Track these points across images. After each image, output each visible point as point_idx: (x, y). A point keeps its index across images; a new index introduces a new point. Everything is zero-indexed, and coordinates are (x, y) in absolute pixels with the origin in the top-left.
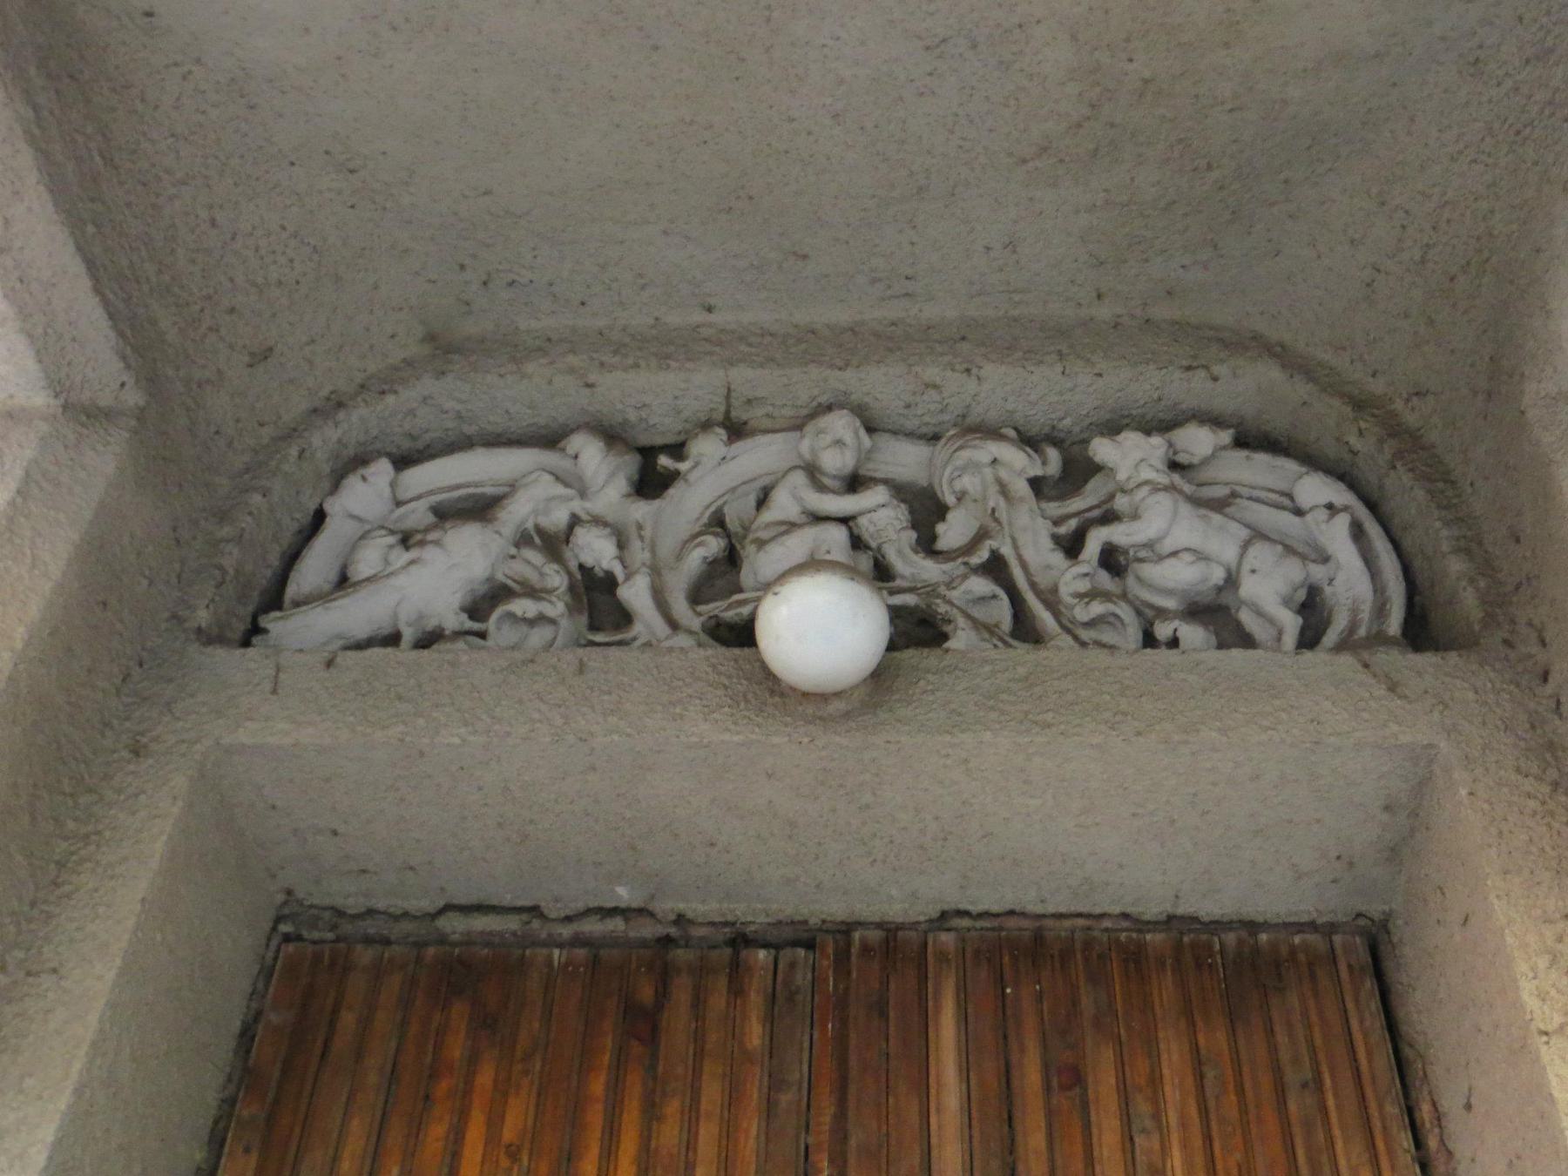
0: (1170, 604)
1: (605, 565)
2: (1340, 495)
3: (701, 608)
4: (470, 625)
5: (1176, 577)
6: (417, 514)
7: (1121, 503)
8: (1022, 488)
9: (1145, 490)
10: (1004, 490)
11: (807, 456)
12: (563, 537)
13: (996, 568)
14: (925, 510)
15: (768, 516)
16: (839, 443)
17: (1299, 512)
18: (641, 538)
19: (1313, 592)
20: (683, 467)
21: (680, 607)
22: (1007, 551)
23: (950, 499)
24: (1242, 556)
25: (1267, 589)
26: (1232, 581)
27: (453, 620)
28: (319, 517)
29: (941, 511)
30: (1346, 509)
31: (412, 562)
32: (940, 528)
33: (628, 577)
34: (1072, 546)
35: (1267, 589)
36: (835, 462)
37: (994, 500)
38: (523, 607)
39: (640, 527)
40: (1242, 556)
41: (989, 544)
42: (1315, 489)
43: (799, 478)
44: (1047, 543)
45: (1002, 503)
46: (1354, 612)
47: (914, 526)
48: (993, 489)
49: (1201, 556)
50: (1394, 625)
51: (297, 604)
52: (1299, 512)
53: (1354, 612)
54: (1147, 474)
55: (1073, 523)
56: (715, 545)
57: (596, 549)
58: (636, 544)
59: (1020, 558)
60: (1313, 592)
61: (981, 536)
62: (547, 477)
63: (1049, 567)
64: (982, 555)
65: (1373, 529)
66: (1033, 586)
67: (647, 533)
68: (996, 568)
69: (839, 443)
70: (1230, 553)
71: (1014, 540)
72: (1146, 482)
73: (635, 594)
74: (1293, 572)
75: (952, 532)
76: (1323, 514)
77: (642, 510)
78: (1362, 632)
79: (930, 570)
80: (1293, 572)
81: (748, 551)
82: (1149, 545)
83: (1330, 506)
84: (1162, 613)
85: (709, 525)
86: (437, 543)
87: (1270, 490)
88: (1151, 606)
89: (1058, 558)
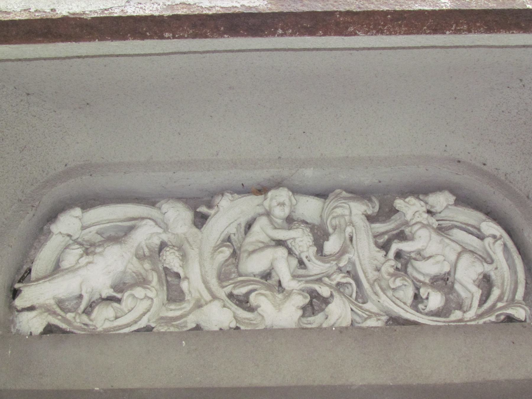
0: (427, 281)
5: (429, 268)
6: (91, 234)
11: (267, 208)
14: (320, 235)
15: (251, 238)
16: (282, 204)
20: (212, 212)
21: (214, 282)
30: (501, 237)
36: (280, 213)
42: (490, 228)
43: (263, 221)
47: (315, 245)
51: (38, 280)
52: (481, 237)
56: (227, 252)
69: (282, 204)
70: (453, 257)
74: (479, 268)
80: (479, 268)
82: (419, 253)
85: (224, 241)
88: (419, 281)
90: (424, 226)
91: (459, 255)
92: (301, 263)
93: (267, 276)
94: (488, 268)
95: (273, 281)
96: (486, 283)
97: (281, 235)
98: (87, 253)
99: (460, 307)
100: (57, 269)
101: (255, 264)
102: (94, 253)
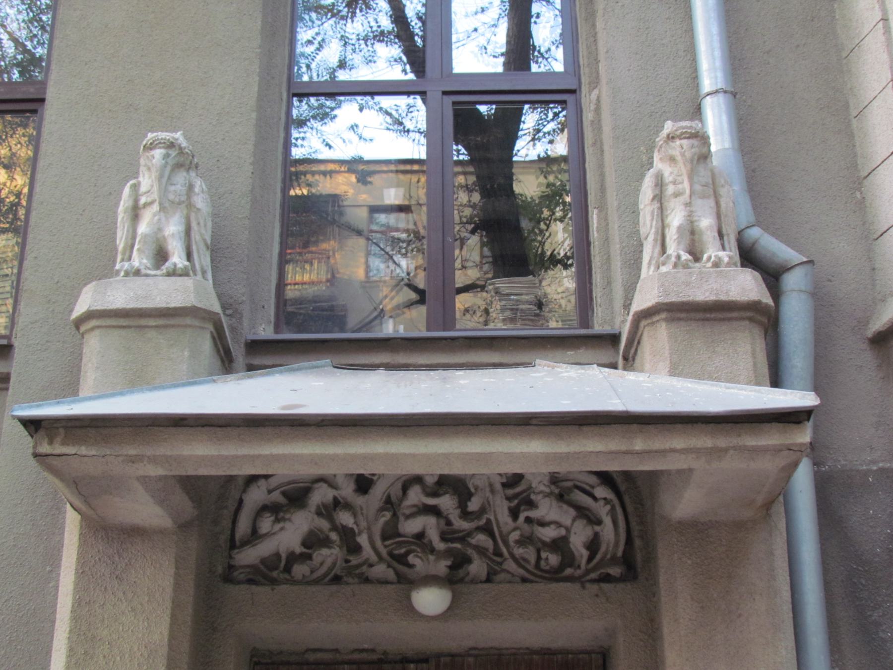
1: (350, 526)
2: (610, 495)
3: (388, 543)
4: (304, 550)
6: (277, 497)
7: (533, 497)
8: (498, 487)
9: (541, 496)
10: (492, 491)
12: (332, 506)
13: (487, 529)
17: (595, 498)
18: (362, 514)
19: (596, 535)
22: (492, 518)
23: (473, 490)
24: (572, 524)
25: (578, 539)
26: (568, 530)
27: (298, 549)
28: (241, 502)
29: (470, 495)
31: (282, 529)
32: (469, 504)
33: (360, 533)
34: (514, 513)
35: (578, 539)
37: (488, 494)
38: (325, 551)
39: (361, 509)
40: (572, 524)
41: (486, 516)
44: (506, 512)
45: (491, 497)
46: (608, 545)
48: (488, 489)
49: (559, 525)
50: (620, 553)
52: (595, 498)
53: (608, 545)
54: (542, 488)
55: (516, 502)
56: (388, 515)
57: (345, 518)
58: (361, 518)
59: (496, 520)
60: (596, 535)
61: (483, 510)
62: (325, 486)
63: (506, 524)
64: (482, 522)
65: (619, 510)
66: (500, 532)
67: (364, 512)
68: (487, 529)
71: (495, 512)
72: (541, 492)
73: (363, 540)
75: (474, 505)
76: (602, 503)
77: (359, 501)
78: (609, 556)
79: (465, 525)
81: (402, 518)
83: (605, 499)
84: (544, 543)
86: (289, 520)
87: (587, 484)
89: (509, 520)
90: (548, 495)
91: (574, 520)
92: (449, 523)
93: (420, 536)
94: (597, 528)
95: (425, 541)
96: (593, 545)
97: (431, 501)
98: (277, 520)
99: (570, 566)
100: (255, 536)
101: (412, 526)
102: (284, 519)
